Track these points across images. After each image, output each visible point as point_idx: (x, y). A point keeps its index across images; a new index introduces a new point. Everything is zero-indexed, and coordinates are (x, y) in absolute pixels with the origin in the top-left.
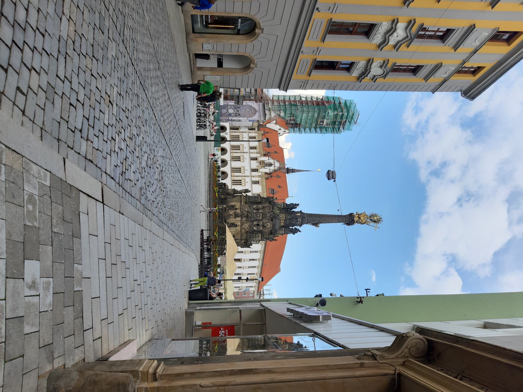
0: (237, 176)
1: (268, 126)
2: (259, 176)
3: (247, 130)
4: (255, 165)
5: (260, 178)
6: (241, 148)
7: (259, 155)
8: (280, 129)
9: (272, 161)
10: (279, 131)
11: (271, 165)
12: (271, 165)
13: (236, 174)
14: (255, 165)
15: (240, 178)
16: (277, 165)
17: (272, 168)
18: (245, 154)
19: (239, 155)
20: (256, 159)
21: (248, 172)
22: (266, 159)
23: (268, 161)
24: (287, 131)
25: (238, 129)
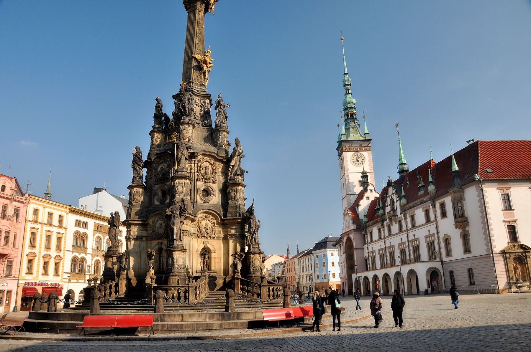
0: (410, 255)
1: (361, 216)
2: (406, 219)
3: (365, 247)
4: (395, 228)
5: (408, 215)
6: (381, 252)
7: (385, 222)
8: (368, 198)
9: (389, 200)
10: (372, 198)
11: (393, 202)
12: (393, 202)
13: (408, 258)
14: (395, 228)
15: (411, 248)
16: (391, 190)
17: (395, 197)
18: (387, 246)
19: (388, 254)
20: (389, 227)
21: (404, 237)
22: (387, 209)
23: (389, 207)
24: (370, 187)
25: (366, 260)
